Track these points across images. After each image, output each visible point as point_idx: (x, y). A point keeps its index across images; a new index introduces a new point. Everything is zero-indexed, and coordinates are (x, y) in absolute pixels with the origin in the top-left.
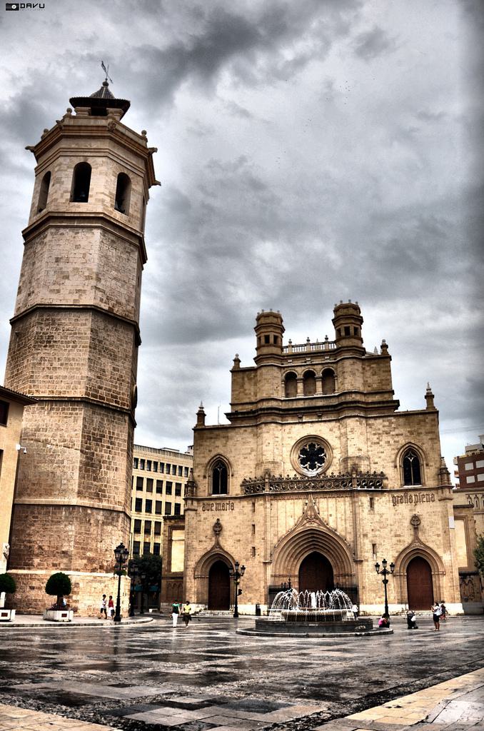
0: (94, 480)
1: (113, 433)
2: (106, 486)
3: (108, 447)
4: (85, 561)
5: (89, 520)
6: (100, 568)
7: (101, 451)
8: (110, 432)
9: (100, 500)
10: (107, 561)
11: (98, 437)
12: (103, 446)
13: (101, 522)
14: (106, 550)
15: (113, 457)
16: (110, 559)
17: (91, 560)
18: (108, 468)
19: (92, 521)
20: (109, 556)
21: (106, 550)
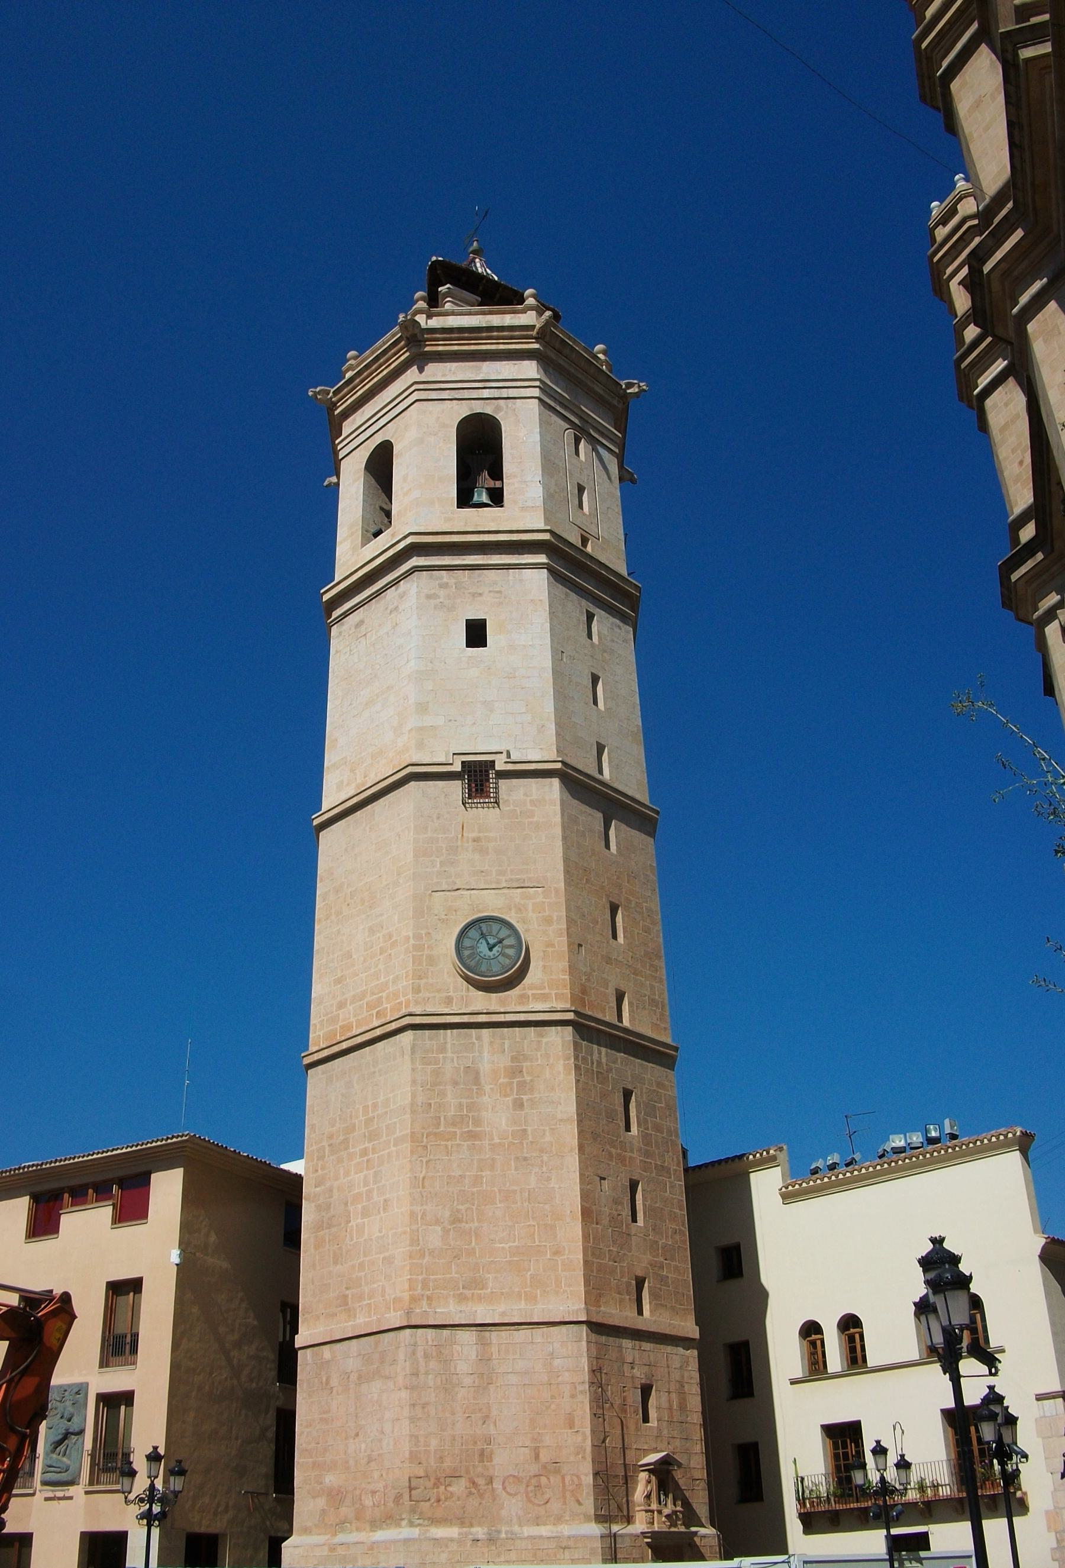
0: (336, 1263)
1: (375, 1106)
2: (361, 1266)
3: (364, 1152)
4: (321, 1502)
5: (327, 1383)
6: (357, 1518)
7: (347, 1173)
8: (366, 1108)
9: (350, 1313)
10: (374, 1492)
11: (341, 1138)
12: (351, 1157)
13: (354, 1377)
14: (370, 1460)
15: (376, 1174)
16: (380, 1486)
17: (336, 1497)
18: (365, 1213)
19: (334, 1382)
20: (376, 1475)
21: (370, 1460)
